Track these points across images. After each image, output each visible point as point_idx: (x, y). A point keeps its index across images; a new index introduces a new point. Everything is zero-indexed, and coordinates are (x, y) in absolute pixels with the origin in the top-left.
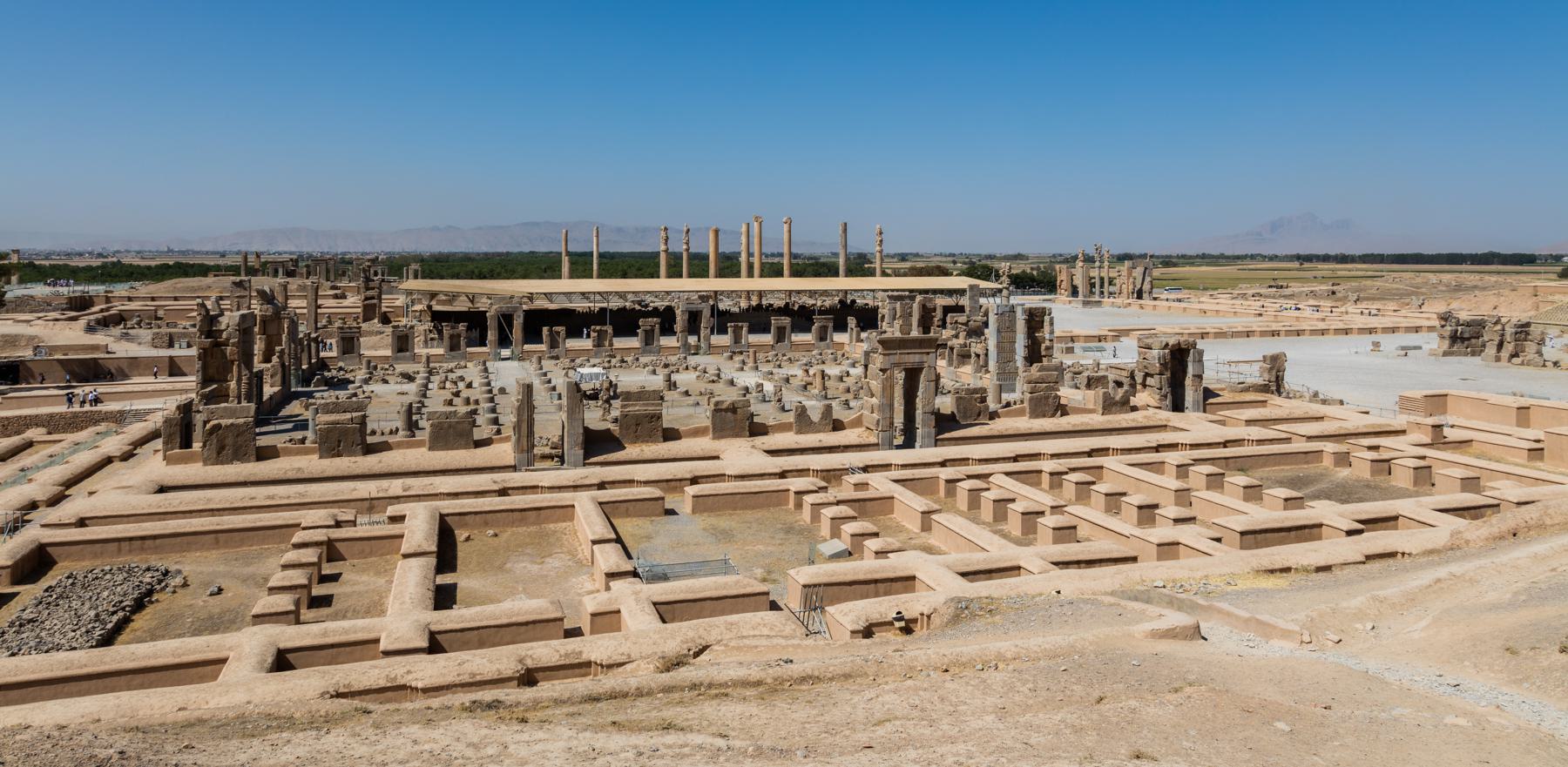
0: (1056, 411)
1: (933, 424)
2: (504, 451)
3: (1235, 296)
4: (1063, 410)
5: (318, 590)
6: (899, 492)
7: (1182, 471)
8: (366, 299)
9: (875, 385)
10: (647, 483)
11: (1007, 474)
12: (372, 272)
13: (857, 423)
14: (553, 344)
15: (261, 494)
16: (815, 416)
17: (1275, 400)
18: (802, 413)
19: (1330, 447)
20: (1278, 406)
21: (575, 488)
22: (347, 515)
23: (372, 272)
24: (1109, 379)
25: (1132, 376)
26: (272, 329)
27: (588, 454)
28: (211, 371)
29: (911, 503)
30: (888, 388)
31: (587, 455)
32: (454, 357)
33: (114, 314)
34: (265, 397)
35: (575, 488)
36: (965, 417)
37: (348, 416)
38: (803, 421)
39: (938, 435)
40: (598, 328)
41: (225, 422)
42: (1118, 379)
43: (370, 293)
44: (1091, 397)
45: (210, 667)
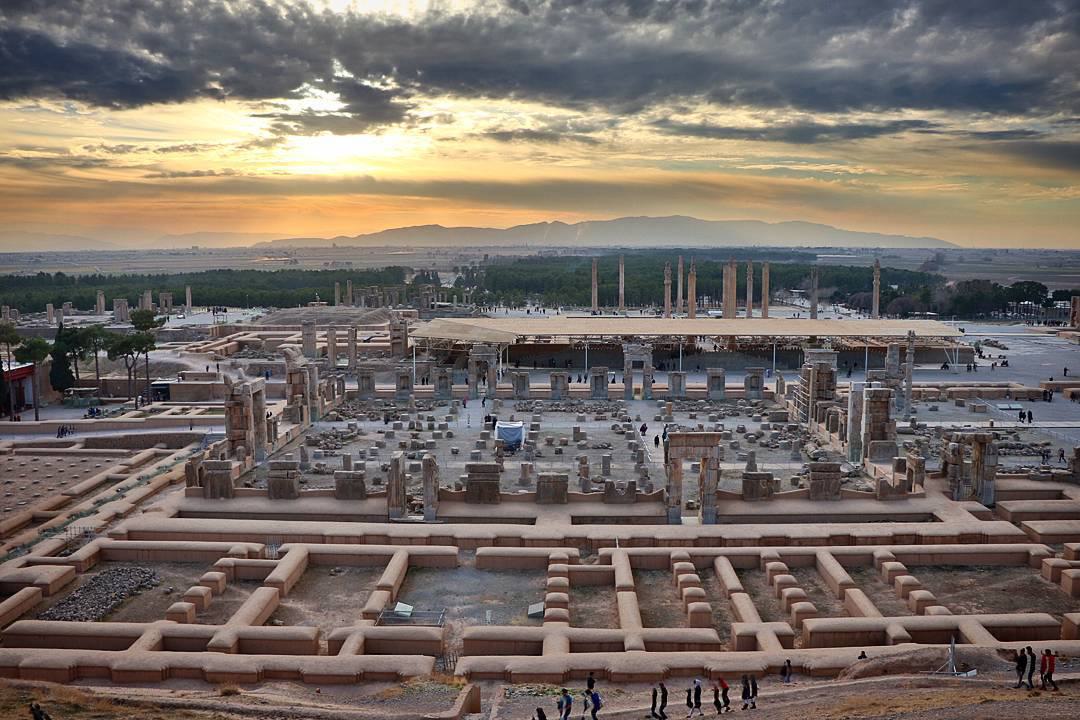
0: (837, 493)
8: (394, 338)
22: (257, 547)
34: (279, 436)
37: (285, 472)
41: (216, 472)
43: (396, 334)
45: (124, 642)
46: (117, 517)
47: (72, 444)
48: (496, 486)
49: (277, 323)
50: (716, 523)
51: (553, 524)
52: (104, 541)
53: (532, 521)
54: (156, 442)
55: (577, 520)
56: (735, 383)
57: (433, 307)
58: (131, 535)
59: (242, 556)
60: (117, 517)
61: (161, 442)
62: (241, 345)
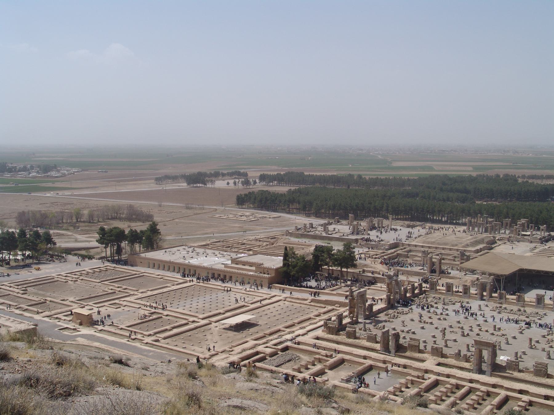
1: (490, 368)
5: (309, 366)
12: (517, 231)
14: (501, 297)
22: (329, 353)
23: (517, 231)
26: (390, 287)
27: (397, 351)
28: (352, 305)
31: (396, 352)
32: (465, 296)
33: (396, 255)
36: (510, 370)
37: (351, 329)
39: (493, 371)
40: (519, 294)
41: (331, 325)
46: (299, 335)
49: (423, 243)
50: (491, 376)
51: (430, 363)
52: (289, 344)
53: (423, 361)
54: (336, 304)
55: (439, 364)
58: (299, 343)
59: (322, 355)
60: (299, 335)
61: (338, 304)
62: (398, 255)
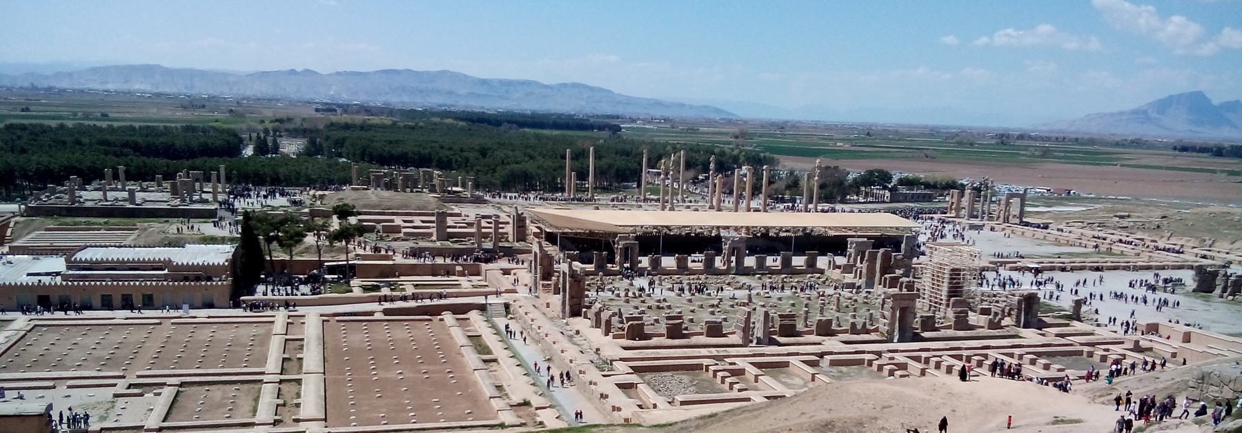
2: (736, 339)
3: (1085, 224)
4: (972, 328)
6: (910, 362)
7: (1021, 357)
9: (887, 314)
10: (869, 352)
11: (949, 356)
13: (876, 330)
15: (679, 352)
16: (859, 327)
17: (1075, 323)
18: (853, 325)
19: (1086, 349)
20: (1077, 326)
21: (789, 354)
24: (992, 310)
25: (1003, 311)
29: (915, 367)
30: (893, 315)
35: (789, 354)
38: (854, 330)
42: (997, 311)
44: (983, 320)
47: (371, 313)
48: (794, 326)
56: (799, 261)
57: (449, 192)
